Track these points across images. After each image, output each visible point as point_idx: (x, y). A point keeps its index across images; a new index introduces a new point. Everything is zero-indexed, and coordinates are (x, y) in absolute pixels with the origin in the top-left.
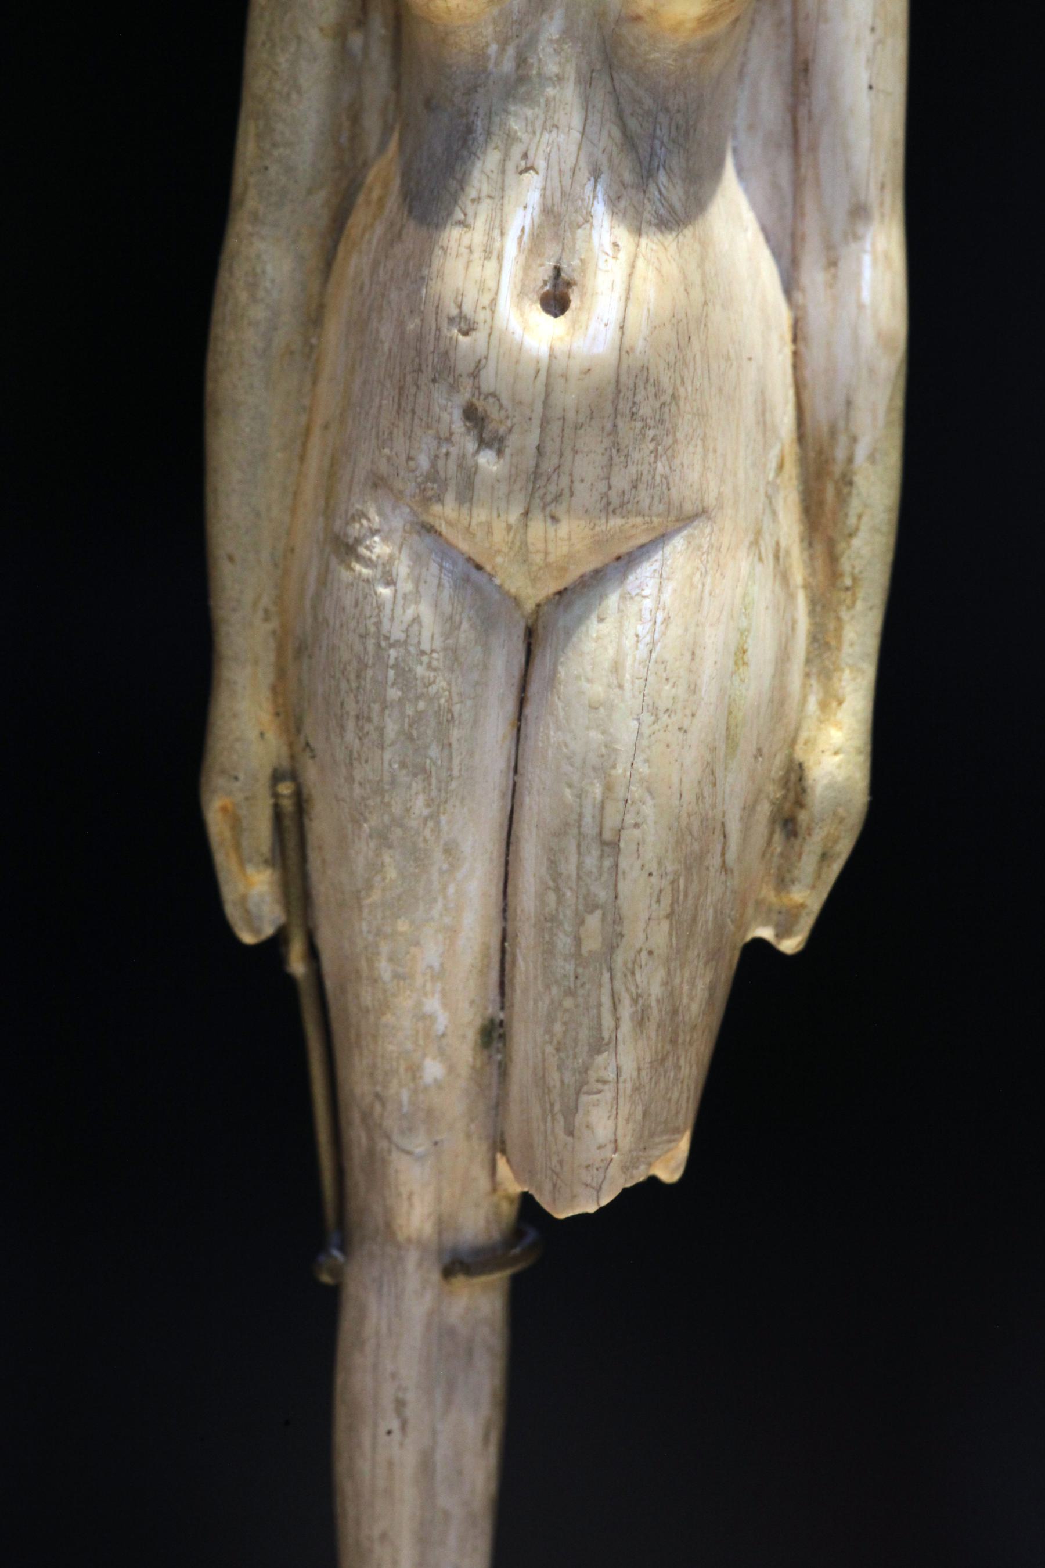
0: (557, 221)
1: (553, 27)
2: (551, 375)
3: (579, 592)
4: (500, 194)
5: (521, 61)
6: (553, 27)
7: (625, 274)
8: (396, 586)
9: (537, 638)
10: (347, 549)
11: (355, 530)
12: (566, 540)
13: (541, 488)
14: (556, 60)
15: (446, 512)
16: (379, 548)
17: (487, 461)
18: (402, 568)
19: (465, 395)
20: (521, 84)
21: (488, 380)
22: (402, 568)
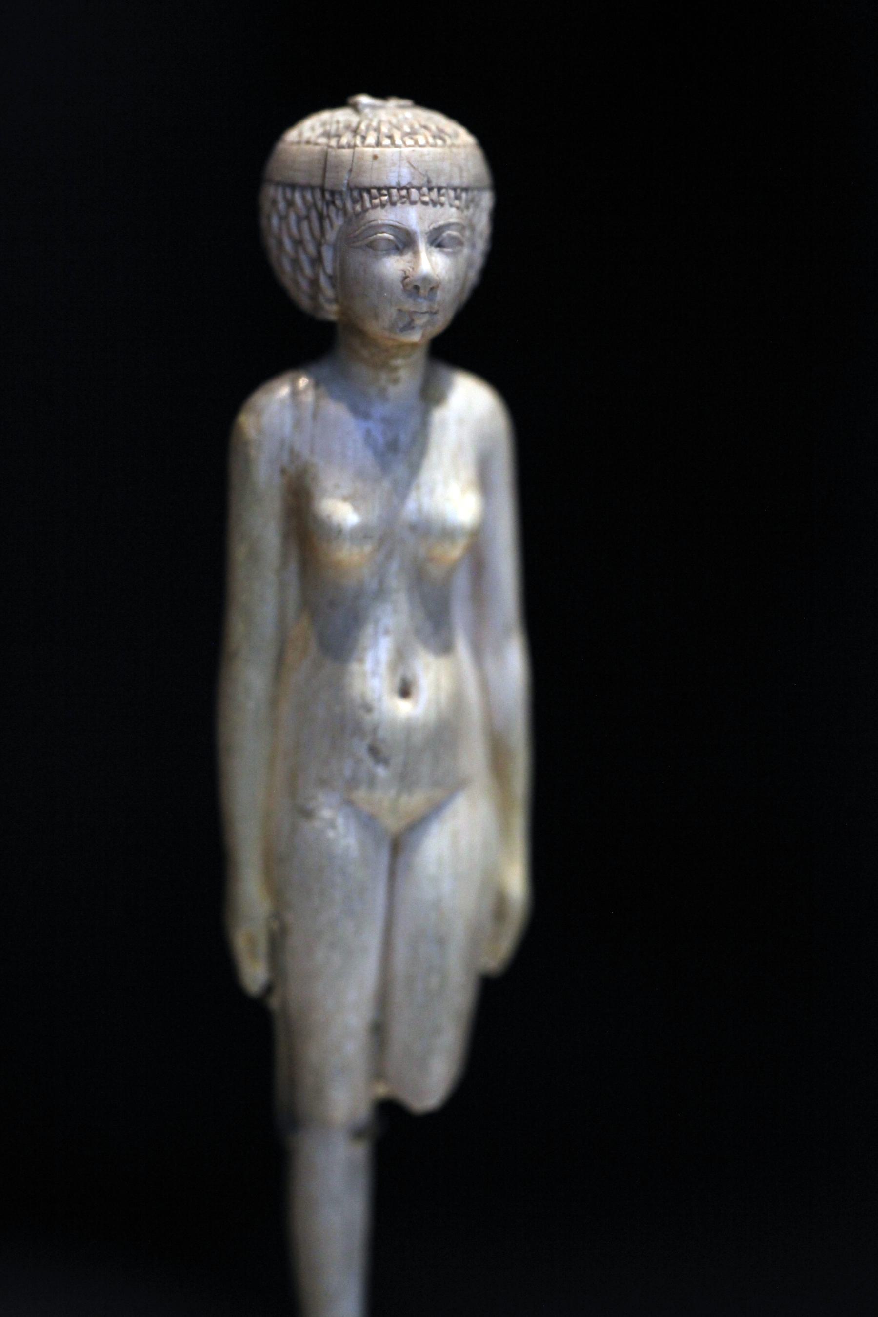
0: (401, 657)
1: (394, 566)
2: (409, 728)
3: (418, 825)
4: (375, 644)
5: (381, 582)
6: (394, 566)
7: (433, 675)
8: (337, 831)
9: (399, 847)
10: (308, 814)
11: (311, 805)
12: (415, 801)
13: (406, 780)
14: (396, 582)
15: (361, 794)
16: (326, 813)
17: (381, 771)
18: (340, 821)
19: (368, 741)
20: (381, 593)
21: (381, 733)
22: (340, 821)
